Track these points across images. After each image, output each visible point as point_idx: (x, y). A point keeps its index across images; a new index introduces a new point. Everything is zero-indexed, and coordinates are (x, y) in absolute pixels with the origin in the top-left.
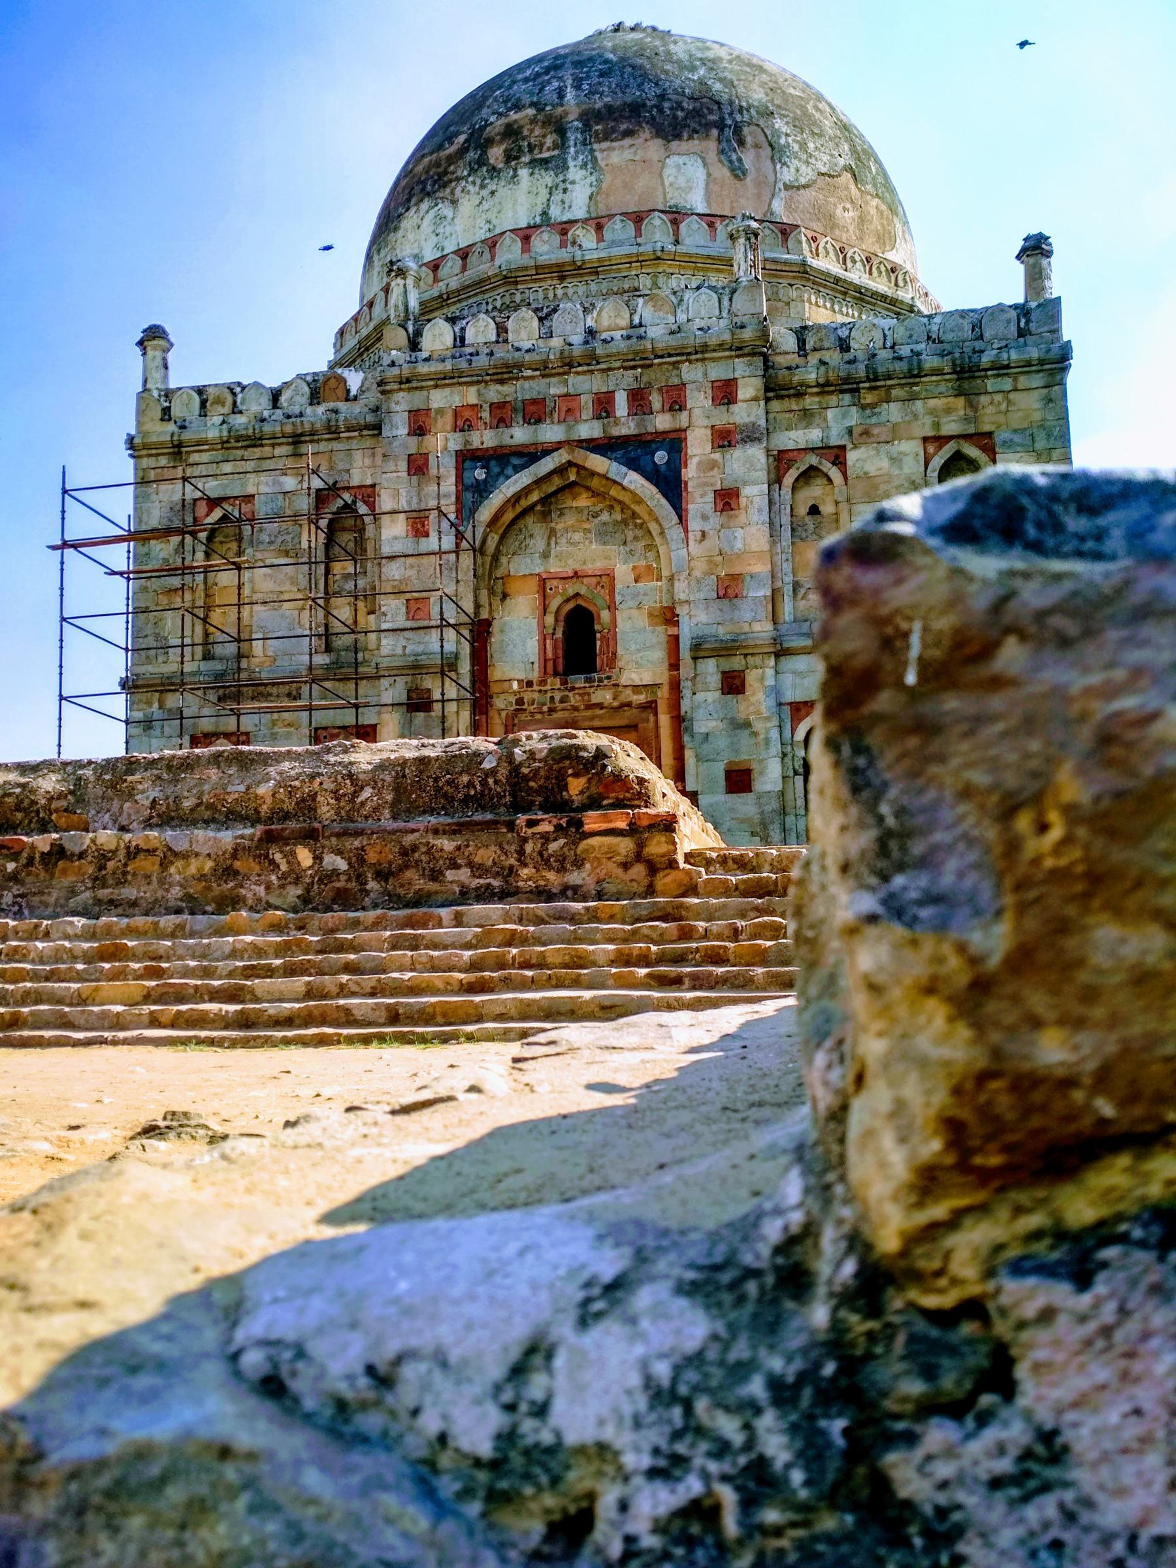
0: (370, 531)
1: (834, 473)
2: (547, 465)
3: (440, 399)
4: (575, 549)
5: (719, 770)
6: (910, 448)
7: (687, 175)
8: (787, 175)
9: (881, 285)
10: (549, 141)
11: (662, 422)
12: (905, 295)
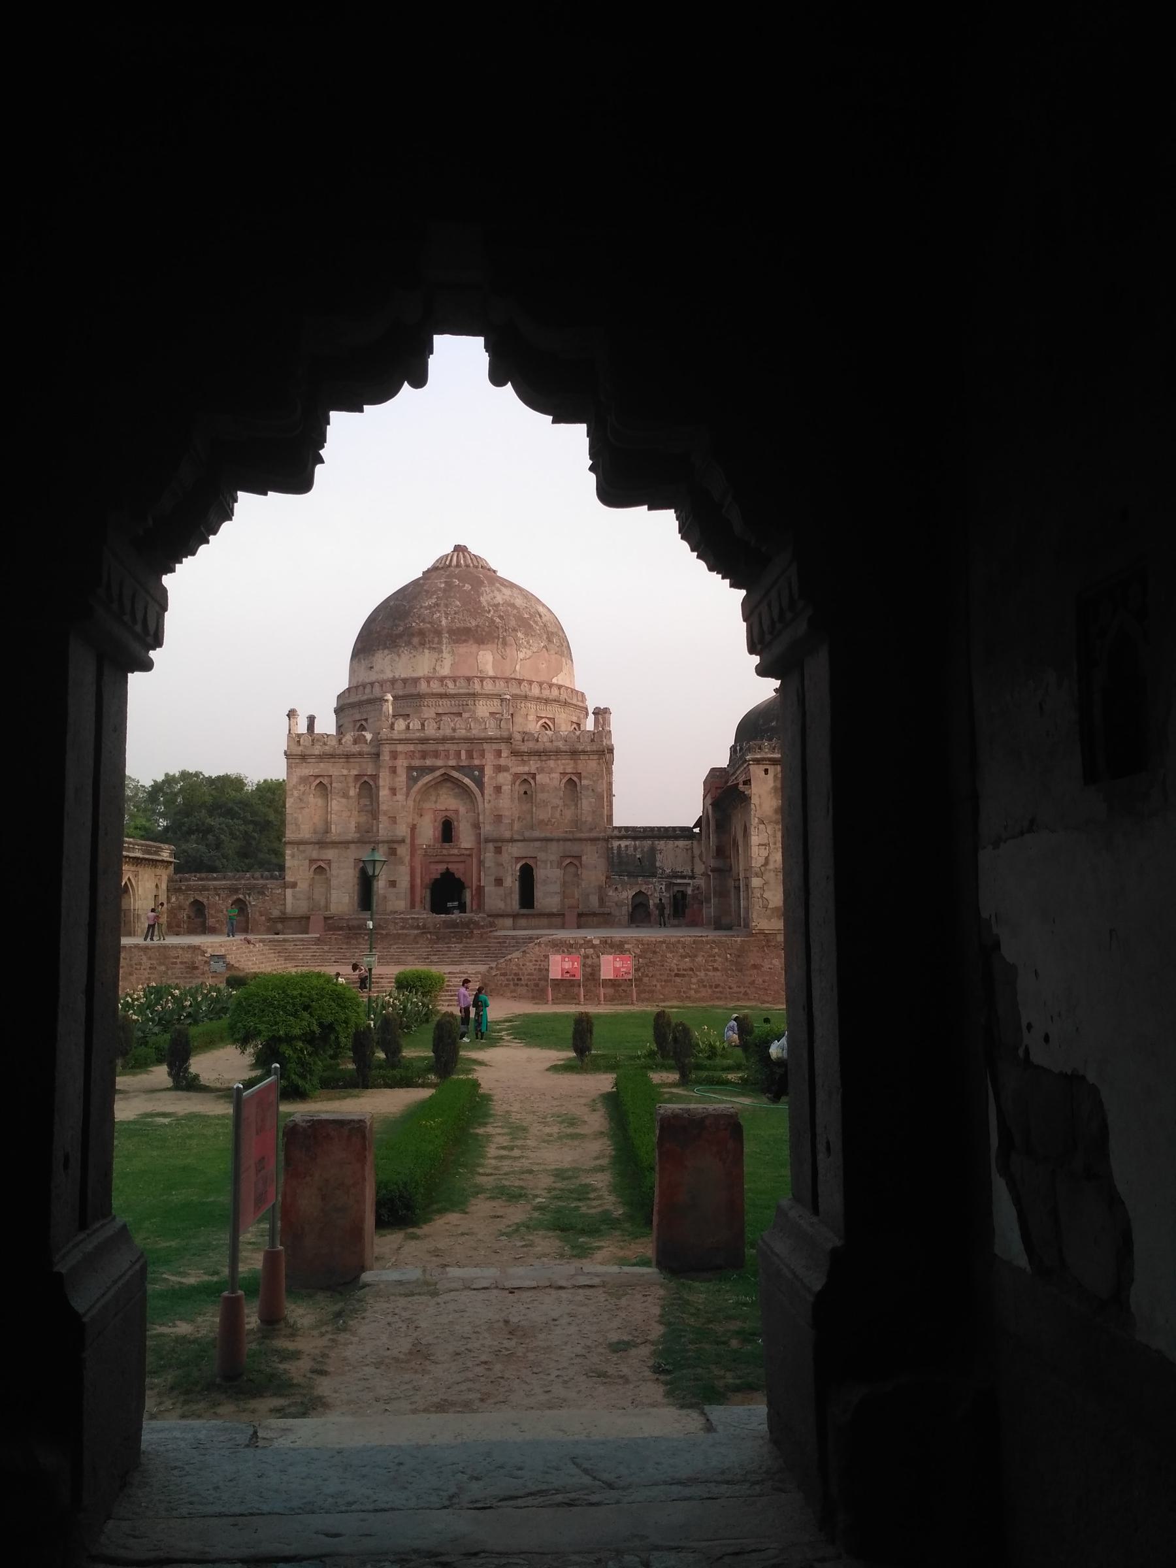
0: (374, 790)
1: (532, 782)
2: (438, 773)
3: (400, 748)
4: (447, 801)
5: (493, 878)
6: (556, 776)
7: (486, 660)
8: (521, 655)
9: (555, 692)
10: (436, 640)
11: (476, 762)
12: (562, 698)
